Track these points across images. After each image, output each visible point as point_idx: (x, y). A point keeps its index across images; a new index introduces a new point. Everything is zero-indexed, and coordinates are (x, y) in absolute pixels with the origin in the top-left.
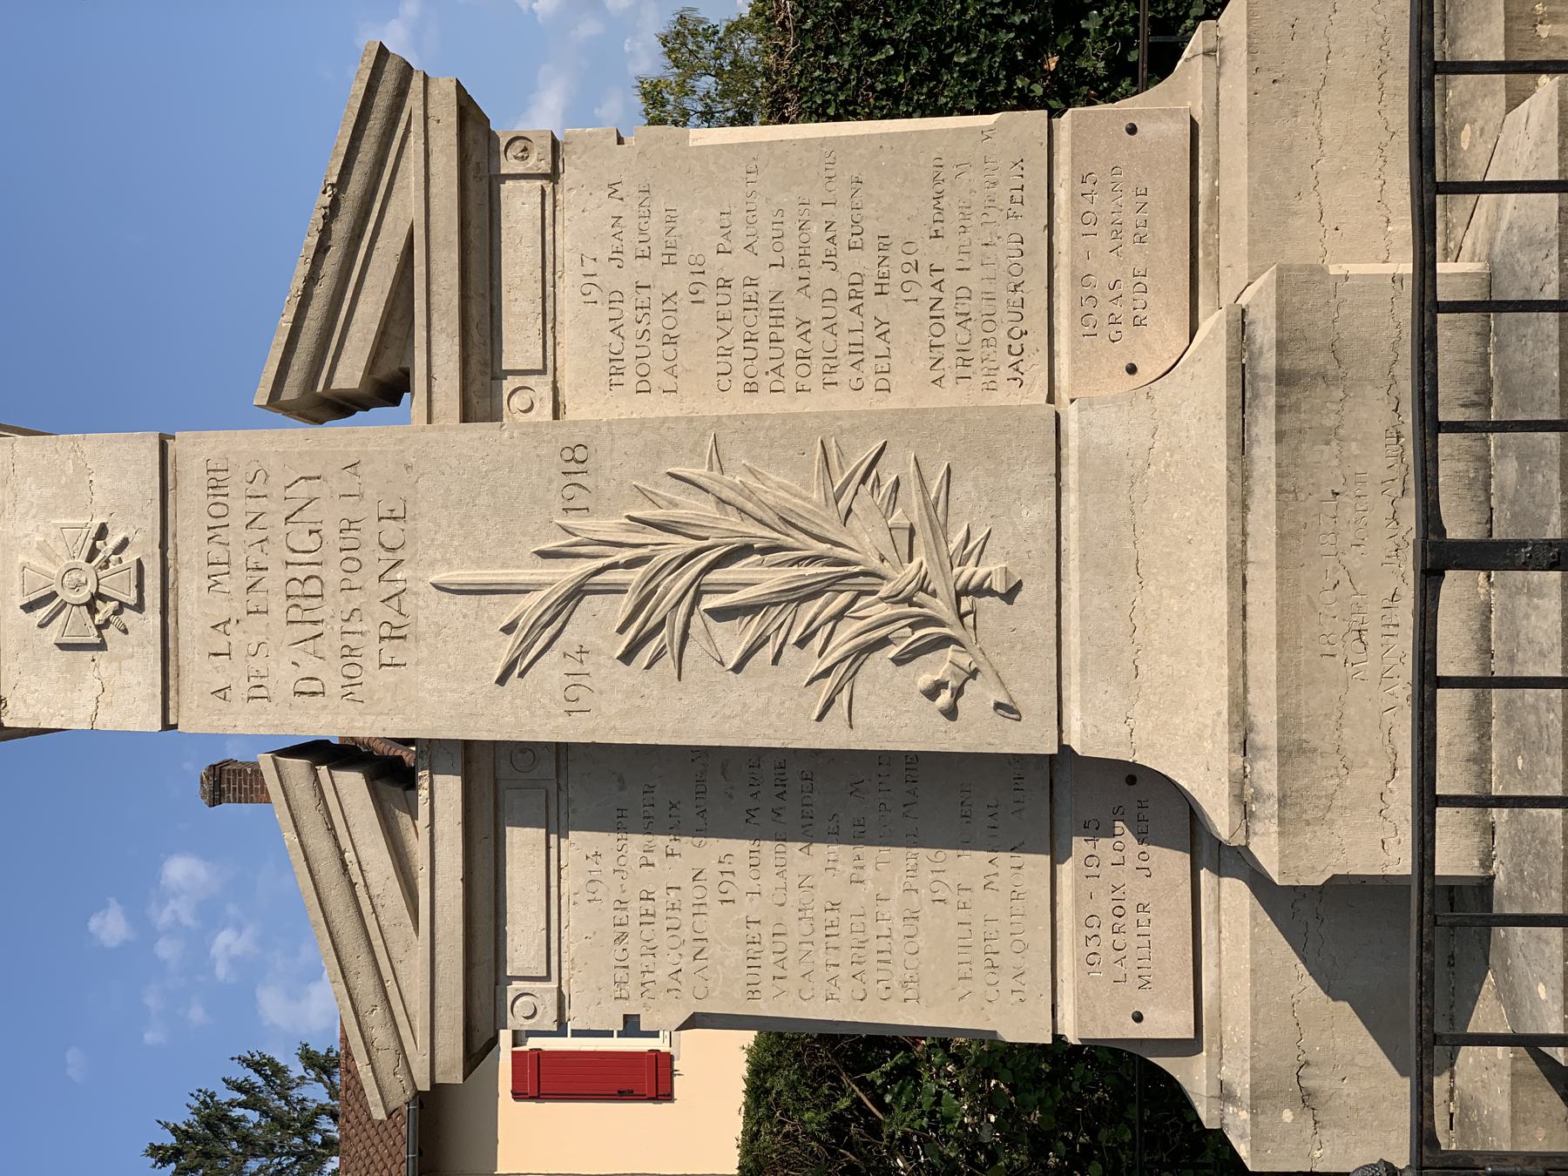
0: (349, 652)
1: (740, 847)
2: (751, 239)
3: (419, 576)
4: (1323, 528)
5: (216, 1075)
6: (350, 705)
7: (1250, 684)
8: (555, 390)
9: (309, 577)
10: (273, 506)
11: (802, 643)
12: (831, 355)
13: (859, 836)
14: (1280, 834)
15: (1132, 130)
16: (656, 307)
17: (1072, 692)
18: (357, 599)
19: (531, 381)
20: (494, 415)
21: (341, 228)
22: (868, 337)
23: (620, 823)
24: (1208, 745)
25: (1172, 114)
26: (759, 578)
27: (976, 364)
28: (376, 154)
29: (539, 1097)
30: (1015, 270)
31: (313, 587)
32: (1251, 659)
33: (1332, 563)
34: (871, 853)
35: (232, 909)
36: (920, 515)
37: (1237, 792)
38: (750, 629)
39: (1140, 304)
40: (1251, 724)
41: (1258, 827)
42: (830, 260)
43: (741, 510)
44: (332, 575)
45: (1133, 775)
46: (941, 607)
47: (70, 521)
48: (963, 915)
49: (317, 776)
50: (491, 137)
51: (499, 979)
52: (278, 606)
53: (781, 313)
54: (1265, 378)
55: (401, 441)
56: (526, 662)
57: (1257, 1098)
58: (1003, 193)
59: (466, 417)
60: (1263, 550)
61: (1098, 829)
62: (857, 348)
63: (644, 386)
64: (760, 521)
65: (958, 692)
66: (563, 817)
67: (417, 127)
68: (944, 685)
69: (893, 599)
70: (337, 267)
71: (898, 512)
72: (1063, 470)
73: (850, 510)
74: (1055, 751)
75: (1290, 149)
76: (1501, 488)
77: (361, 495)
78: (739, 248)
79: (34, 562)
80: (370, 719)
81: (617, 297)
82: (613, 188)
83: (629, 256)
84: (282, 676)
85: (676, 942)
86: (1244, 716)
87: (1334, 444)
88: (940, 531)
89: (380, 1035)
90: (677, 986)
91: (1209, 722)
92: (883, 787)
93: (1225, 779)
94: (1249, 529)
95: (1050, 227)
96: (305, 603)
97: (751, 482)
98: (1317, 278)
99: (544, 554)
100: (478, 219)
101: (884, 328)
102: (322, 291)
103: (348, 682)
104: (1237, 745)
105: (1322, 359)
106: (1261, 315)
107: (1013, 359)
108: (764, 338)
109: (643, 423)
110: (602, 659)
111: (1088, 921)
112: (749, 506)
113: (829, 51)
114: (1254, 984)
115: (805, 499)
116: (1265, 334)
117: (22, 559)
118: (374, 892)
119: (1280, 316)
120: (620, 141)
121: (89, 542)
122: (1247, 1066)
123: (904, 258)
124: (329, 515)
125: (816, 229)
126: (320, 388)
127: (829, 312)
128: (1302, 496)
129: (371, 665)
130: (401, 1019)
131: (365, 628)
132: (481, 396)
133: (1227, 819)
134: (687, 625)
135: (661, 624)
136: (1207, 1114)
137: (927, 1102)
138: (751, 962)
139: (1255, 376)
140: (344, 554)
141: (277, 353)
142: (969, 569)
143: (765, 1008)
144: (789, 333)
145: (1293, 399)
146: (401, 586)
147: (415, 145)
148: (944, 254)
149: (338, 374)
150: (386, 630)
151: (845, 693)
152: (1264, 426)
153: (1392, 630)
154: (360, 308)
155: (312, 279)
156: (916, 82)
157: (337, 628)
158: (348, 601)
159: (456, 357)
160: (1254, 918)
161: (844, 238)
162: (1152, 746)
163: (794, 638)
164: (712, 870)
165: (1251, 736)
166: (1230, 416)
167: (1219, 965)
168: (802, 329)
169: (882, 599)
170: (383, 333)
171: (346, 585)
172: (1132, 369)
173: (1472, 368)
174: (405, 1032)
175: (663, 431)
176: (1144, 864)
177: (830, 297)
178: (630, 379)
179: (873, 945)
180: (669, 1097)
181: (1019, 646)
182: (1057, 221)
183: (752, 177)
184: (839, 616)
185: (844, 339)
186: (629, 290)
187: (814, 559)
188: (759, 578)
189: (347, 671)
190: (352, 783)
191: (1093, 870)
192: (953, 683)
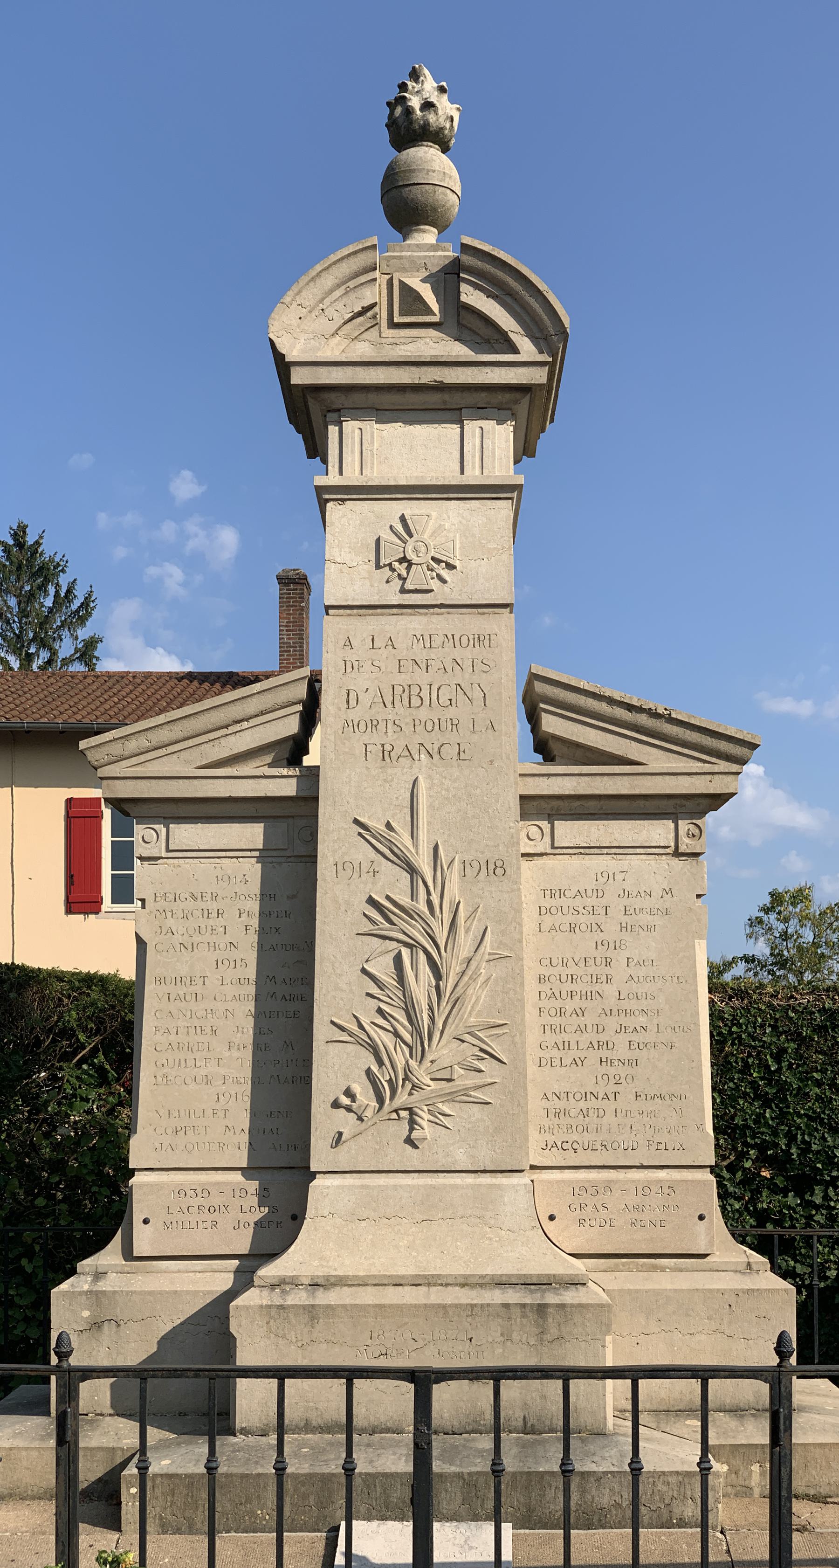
1: (251, 972)
2: (636, 979)
3: (423, 765)
4: (450, 1332)
5: (79, 576)
6: (340, 725)
8: (541, 855)
10: (467, 676)
11: (380, 1011)
12: (562, 1029)
13: (258, 1047)
14: (261, 1306)
16: (592, 919)
17: (349, 1180)
19: (547, 839)
20: (524, 815)
21: (643, 720)
22: (574, 1053)
23: (267, 896)
24: (316, 1263)
25: (711, 1243)
26: (421, 984)
27: (556, 1121)
28: (689, 742)
29: (68, 817)
30: (615, 1145)
31: (415, 701)
32: (369, 1288)
33: (428, 1337)
34: (248, 1055)
35: (199, 578)
36: (459, 1085)
37: (287, 1280)
38: (388, 977)
39: (593, 1223)
40: (329, 1289)
41: (266, 1292)
42: (623, 1029)
43: (463, 973)
44: (423, 714)
45: (297, 1218)
46: (402, 1098)
47: (458, 546)
48: (209, 1112)
49: (296, 703)
50: (702, 814)
51: (168, 819)
52: (403, 679)
53: (589, 998)
54: (543, 1297)
55: (508, 758)
56: (368, 837)
57: (97, 1295)
58: (664, 1137)
59: (522, 797)
61: (263, 1197)
62: (566, 1045)
63: (543, 911)
64: (456, 985)
65: (349, 1109)
66: (270, 859)
67: (707, 768)
68: (353, 1101)
69: (407, 1069)
70: (618, 717)
71: (462, 1072)
72: (488, 1174)
73: (463, 1041)
74: (312, 1169)
75: (687, 1315)
76: (473, 1440)
77: (474, 732)
78: (630, 971)
79: (431, 523)
80: (332, 738)
81: (600, 894)
82: (669, 892)
83: (625, 901)
84: (360, 682)
85: (191, 932)
86: (334, 1285)
87: (502, 1339)
88: (451, 1098)
89: (132, 745)
90: (164, 933)
91: (330, 1264)
92: (289, 1062)
93: (294, 1273)
94: (450, 1288)
95: (642, 1167)
97: (481, 980)
98: (604, 1328)
99: (436, 848)
100: (650, 806)
101: (579, 1063)
102: (603, 708)
103: (355, 724)
104: (316, 1280)
105: (554, 1332)
106: (581, 1294)
107: (559, 1144)
109: (519, 911)
110: (370, 885)
111: (206, 1190)
112: (466, 978)
113: (774, 1027)
114: (167, 1292)
115: (470, 1013)
116: (570, 1297)
117: (434, 514)
118: (222, 740)
119: (581, 1306)
120: (699, 896)
121: (444, 559)
122: (117, 1289)
123: (623, 1076)
124: (462, 712)
125: (643, 1020)
126: (542, 705)
127: (589, 1029)
128: (469, 1319)
129: (366, 739)
130: (142, 758)
131: (389, 734)
132: (534, 807)
133: (270, 1274)
134: (391, 939)
135: (391, 923)
136: (86, 1265)
137: (83, 1091)
138: (179, 979)
139: (544, 1291)
141: (564, 679)
142: (426, 1116)
143: (150, 988)
144: (577, 1003)
146: (416, 757)
147: (696, 766)
148: (626, 1101)
149: (551, 717)
150: (388, 748)
151: (347, 1038)
152: (513, 1296)
154: (593, 731)
155: (611, 701)
156: (753, 1084)
157: (390, 717)
158: (407, 724)
159: (561, 792)
160: (209, 1292)
161: (635, 1037)
162: (316, 1229)
163: (384, 1007)
164: (236, 955)
165: (321, 1289)
166: (519, 1276)
167: (179, 1272)
168: (579, 1011)
169: (407, 1062)
170: (578, 745)
171: (417, 722)
172: (552, 1218)
173: (547, 1423)
174: (134, 760)
175: (514, 924)
176: (241, 1225)
177: (599, 1029)
178: (548, 903)
179: (190, 1057)
180: (69, 911)
181: (377, 1147)
182: (646, 1171)
183: (675, 979)
184: (396, 1034)
185: (572, 1038)
186: (604, 902)
187: (432, 1019)
188: (421, 984)
189: (362, 723)
190: (291, 726)
191: (237, 1193)
192: (355, 1106)
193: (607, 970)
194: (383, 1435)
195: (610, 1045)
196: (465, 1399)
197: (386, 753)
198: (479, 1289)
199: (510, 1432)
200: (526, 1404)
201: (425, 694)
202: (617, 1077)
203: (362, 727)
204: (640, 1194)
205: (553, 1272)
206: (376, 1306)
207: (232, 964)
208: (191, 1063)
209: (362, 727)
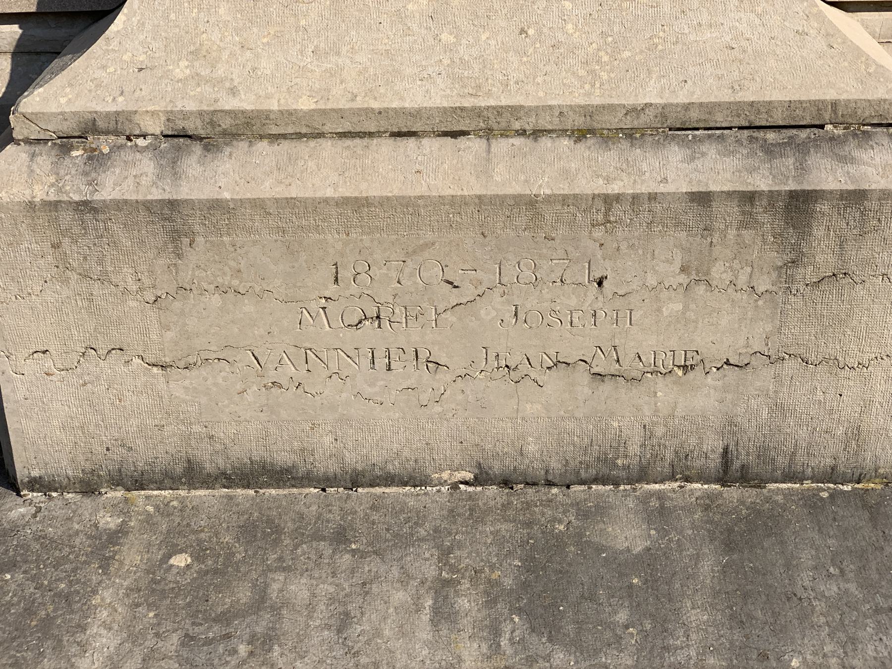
4: (545, 265)
7: (285, 145)
14: (31, 206)
24: (181, 69)
32: (327, 145)
33: (488, 278)
37: (101, 124)
41: (45, 160)
54: (802, 169)
60: (511, 171)
86: (231, 136)
87: (683, 279)
91: (220, 72)
93: (121, 104)
94: (546, 142)
104: (180, 124)
128: (599, 233)
133: (53, 108)
139: (802, 149)
145: (764, 218)
152: (721, 169)
153: (382, 362)
165: (197, 148)
166: (736, 107)
173: (782, 461)
194: (378, 490)
196: (579, 414)
198: (625, 144)
199: (687, 479)
200: (731, 423)
205: (830, 95)
206: (344, 202)
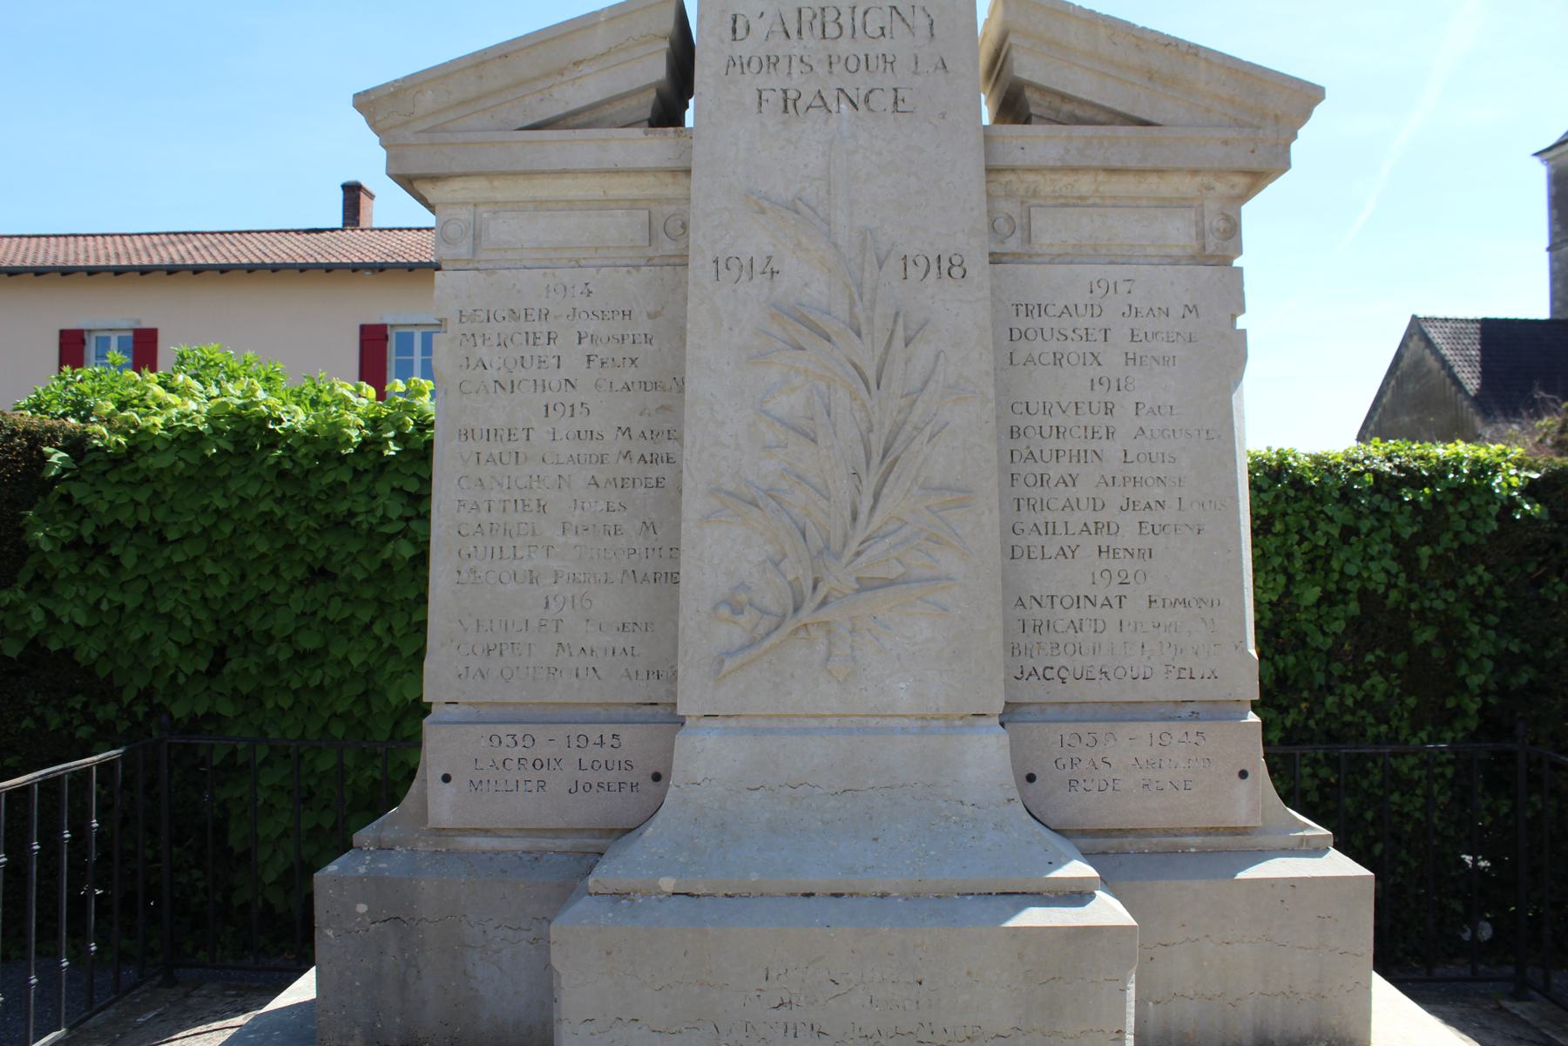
0: (772, 62)
2: (1148, 433)
9: (841, 27)
15: (1243, 774)
16: (1086, 347)
18: (821, 70)
30: (1120, 672)
31: (832, 30)
39: (1088, 785)
42: (1130, 505)
44: (844, 47)
63: (1016, 335)
82: (1192, 309)
96: (817, 24)
101: (1069, 554)
103: (745, 61)
107: (1040, 671)
108: (1060, 444)
125: (1158, 492)
127: (1083, 505)
140: (862, 58)
146: (834, 108)
150: (792, 95)
161: (1150, 518)
168: (1068, 480)
171: (834, 59)
177: (1096, 505)
183: (1204, 434)
190: (656, 69)
191: (574, 742)
193: (1108, 420)
195: (1113, 528)
197: (790, 104)
201: (845, 20)
202: (1123, 574)
203: (755, 65)
204: (1156, 745)
207: (568, 412)
208: (508, 552)
209: (755, 65)
